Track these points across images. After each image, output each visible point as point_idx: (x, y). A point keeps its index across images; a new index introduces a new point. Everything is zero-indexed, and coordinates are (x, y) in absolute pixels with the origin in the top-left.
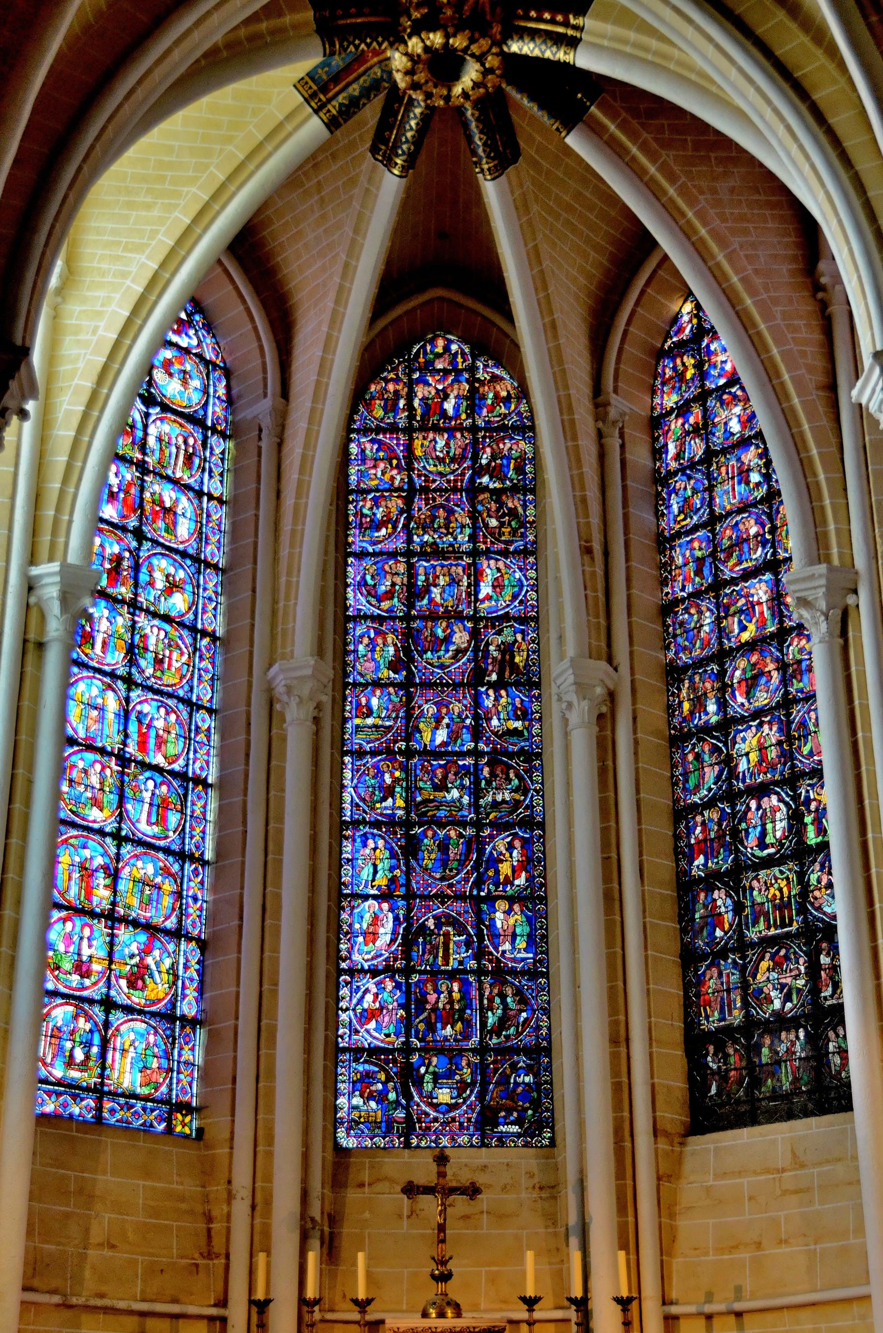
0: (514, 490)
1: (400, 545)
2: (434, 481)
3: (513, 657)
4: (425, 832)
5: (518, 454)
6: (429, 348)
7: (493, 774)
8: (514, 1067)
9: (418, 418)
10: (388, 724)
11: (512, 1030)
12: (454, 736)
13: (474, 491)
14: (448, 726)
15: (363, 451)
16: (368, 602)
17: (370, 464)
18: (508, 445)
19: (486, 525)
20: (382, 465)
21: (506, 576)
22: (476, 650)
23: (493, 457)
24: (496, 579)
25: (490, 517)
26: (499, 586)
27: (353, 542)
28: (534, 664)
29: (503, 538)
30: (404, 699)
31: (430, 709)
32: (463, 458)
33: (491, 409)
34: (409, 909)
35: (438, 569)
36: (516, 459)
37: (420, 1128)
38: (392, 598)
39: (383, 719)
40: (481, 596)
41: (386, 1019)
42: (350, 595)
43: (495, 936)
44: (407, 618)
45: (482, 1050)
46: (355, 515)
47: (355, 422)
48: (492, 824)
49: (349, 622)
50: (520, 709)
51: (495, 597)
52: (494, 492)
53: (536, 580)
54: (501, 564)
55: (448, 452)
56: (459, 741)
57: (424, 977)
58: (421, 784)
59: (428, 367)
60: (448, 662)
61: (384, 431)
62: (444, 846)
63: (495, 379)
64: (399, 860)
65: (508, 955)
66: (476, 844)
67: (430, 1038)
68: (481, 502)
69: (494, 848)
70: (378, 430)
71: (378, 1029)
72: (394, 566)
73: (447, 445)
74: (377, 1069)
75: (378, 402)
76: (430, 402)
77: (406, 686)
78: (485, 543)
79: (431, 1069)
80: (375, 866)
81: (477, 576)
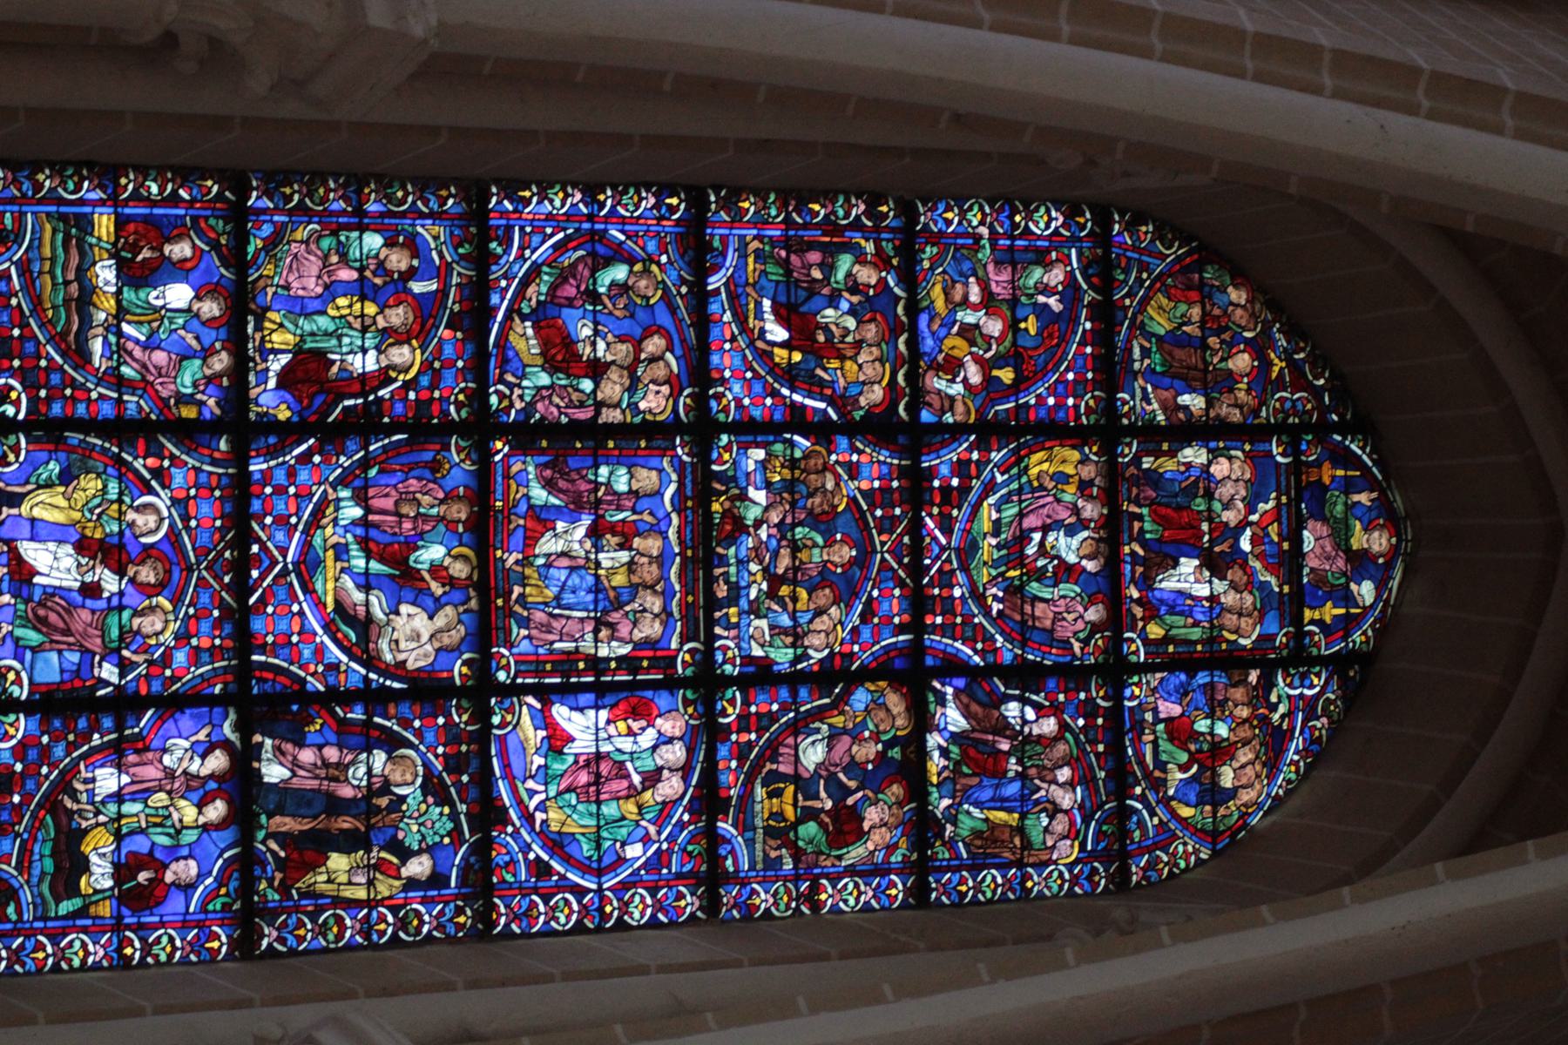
0: (922, 827)
2: (946, 525)
3: (350, 842)
5: (1036, 836)
6: (1363, 498)
9: (1147, 462)
10: (97, 346)
13: (912, 674)
14: (91, 590)
15: (1041, 258)
16: (535, 271)
17: (999, 280)
18: (1066, 800)
19: (800, 727)
20: (994, 327)
21: (630, 807)
22: (374, 698)
23: (1026, 743)
24: (620, 771)
25: (832, 739)
26: (597, 780)
27: (737, 218)
28: (323, 930)
29: (760, 792)
30: (189, 413)
31: (150, 521)
32: (1022, 632)
33: (1179, 731)
35: (653, 545)
36: (1020, 830)
38: (551, 366)
39: (113, 327)
40: (560, 712)
42: (557, 203)
44: (481, 427)
46: (830, 226)
47: (1131, 227)
49: (464, 196)
50: (157, 881)
51: (558, 767)
52: (914, 743)
53: (621, 925)
54: (671, 786)
55: (1040, 575)
56: (32, 637)
59: (1303, 499)
60: (326, 586)
61: (1103, 337)
63: (1275, 741)
68: (877, 704)
70: (1106, 314)
72: (660, 371)
73: (1066, 572)
75: (1196, 312)
76: (1200, 504)
77: (239, 425)
78: (744, 723)
81: (625, 690)
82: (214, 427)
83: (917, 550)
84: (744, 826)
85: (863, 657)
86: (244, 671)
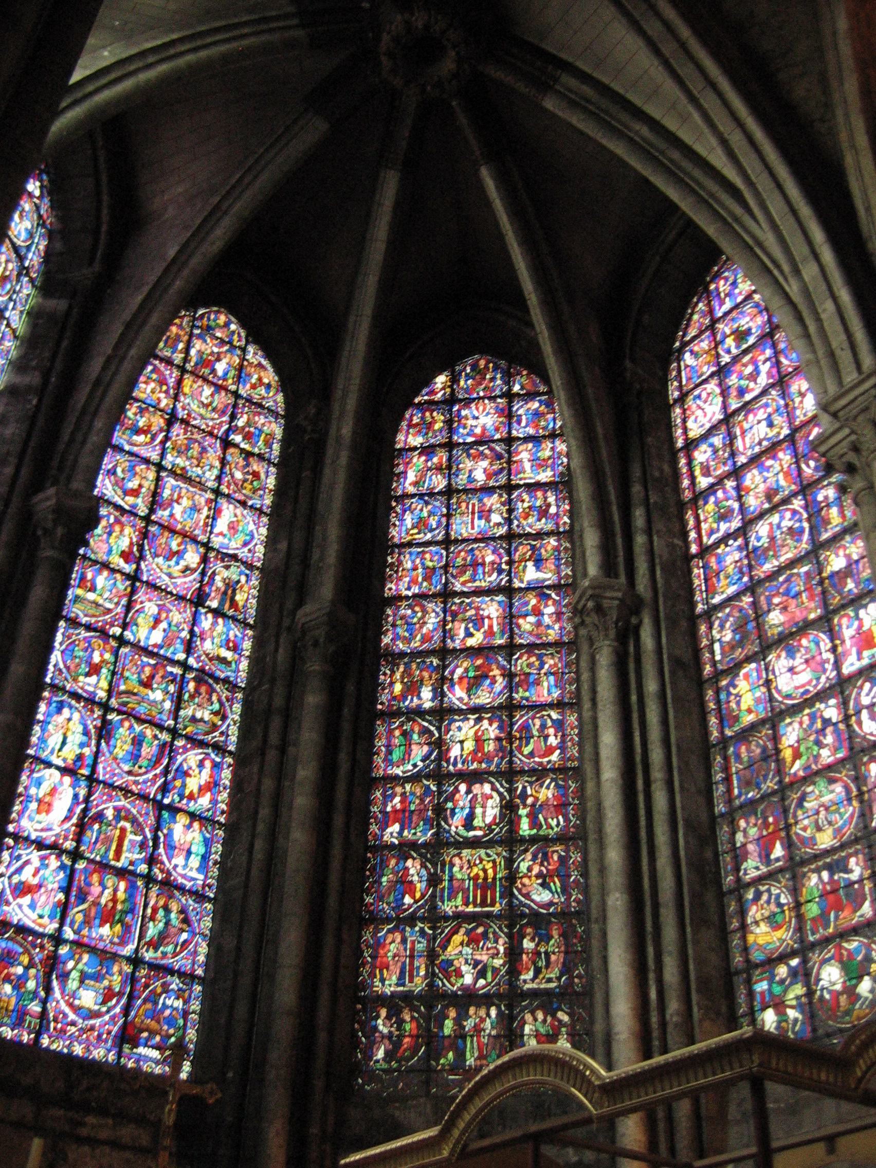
1: (154, 456)
4: (122, 721)
7: (197, 690)
8: (166, 988)
11: (170, 948)
12: (168, 641)
22: (203, 574)
34: (90, 794)
35: (184, 491)
37: (55, 1029)
41: (43, 898)
43: (170, 847)
44: (147, 519)
45: (136, 961)
48: (189, 738)
57: (92, 866)
58: (127, 674)
62: (137, 742)
64: (90, 738)
65: (179, 870)
66: (167, 750)
67: (85, 932)
69: (185, 760)
71: (33, 906)
74: (21, 950)
78: (228, 487)
79: (80, 966)
80: (65, 738)
82: (133, 585)
83: (199, 428)
84: (251, 498)
85: (219, 453)
86: (191, 601)
